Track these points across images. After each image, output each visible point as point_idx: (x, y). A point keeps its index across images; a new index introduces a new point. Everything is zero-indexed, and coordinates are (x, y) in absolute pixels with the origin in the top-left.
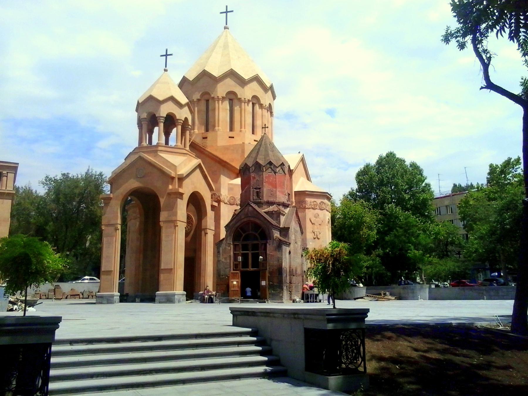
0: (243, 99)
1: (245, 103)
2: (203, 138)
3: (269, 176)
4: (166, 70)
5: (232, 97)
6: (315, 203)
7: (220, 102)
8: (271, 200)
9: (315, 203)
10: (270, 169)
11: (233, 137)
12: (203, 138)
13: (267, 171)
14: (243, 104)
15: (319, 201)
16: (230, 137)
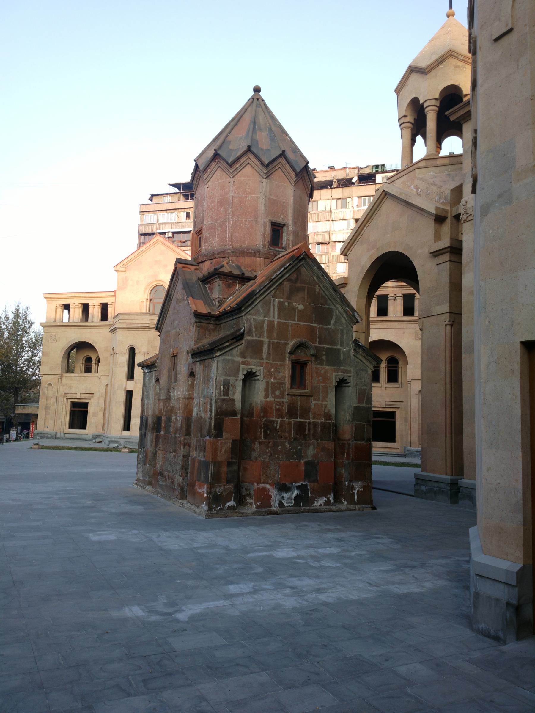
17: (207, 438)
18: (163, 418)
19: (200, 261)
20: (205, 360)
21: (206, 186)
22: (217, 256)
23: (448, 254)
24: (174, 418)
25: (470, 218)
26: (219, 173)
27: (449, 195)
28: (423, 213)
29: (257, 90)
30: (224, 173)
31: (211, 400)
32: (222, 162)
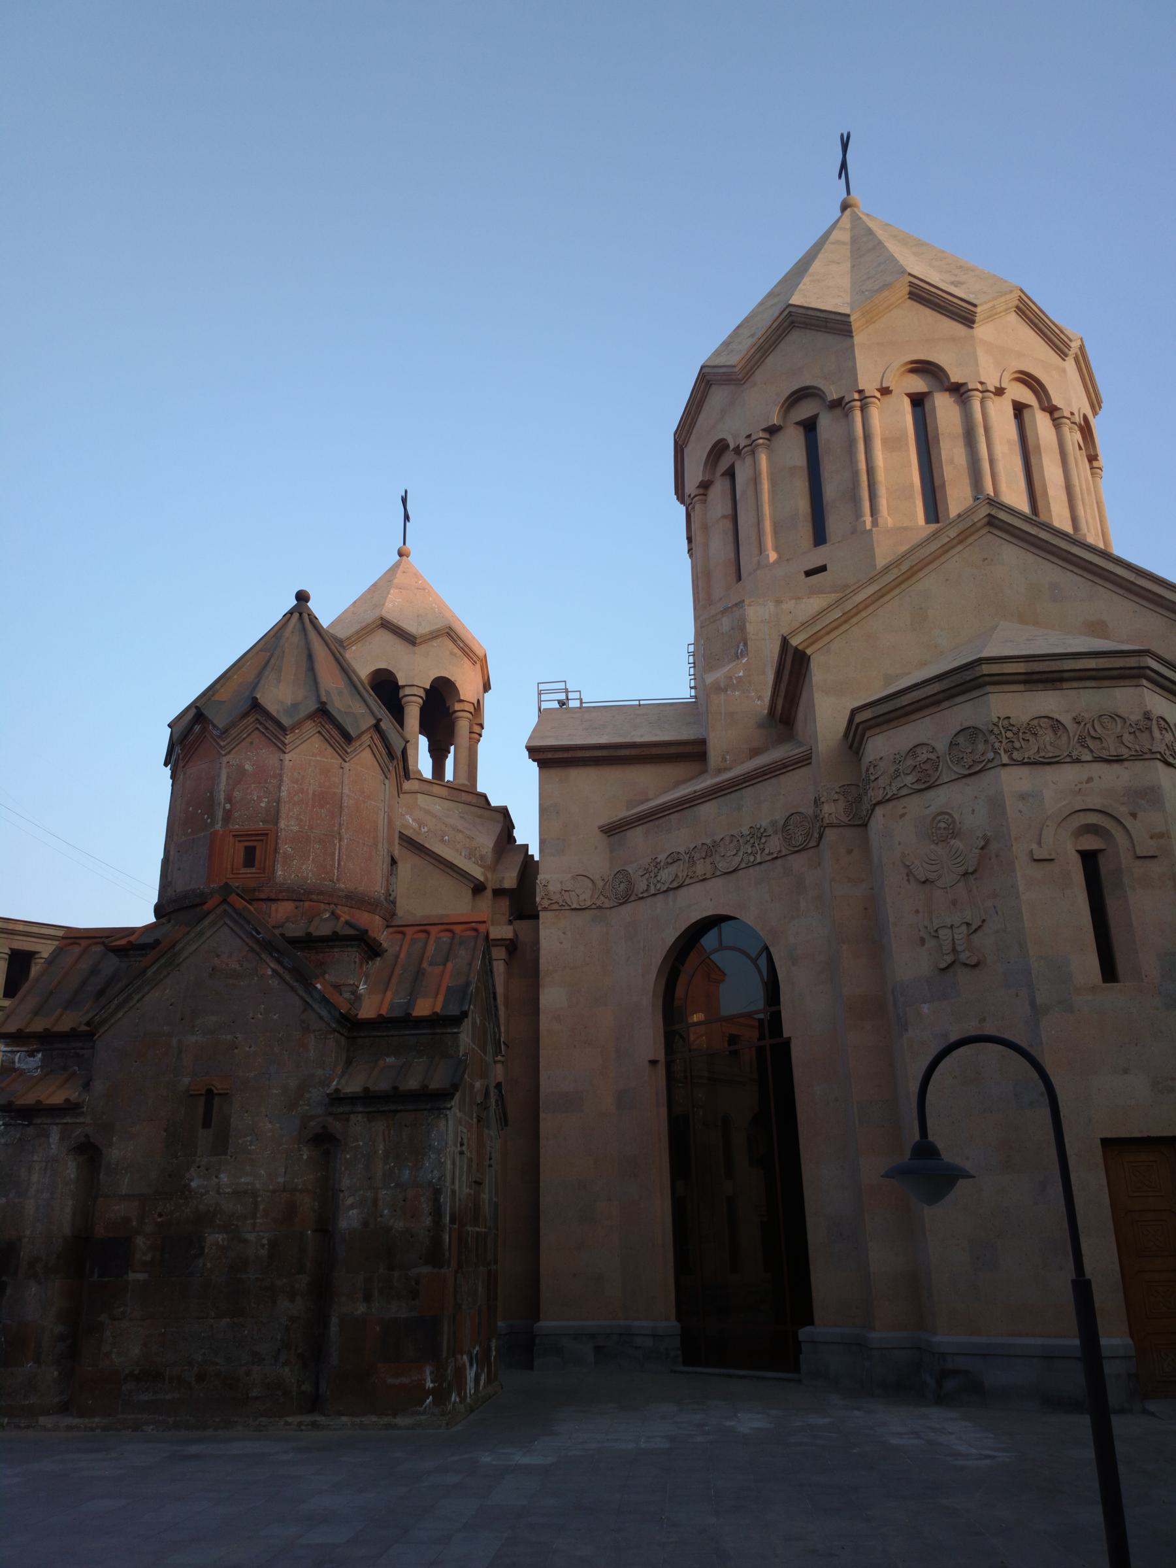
4: (401, 554)
17: (425, 1270)
18: (140, 1241)
19: (262, 896)
20: (401, 1111)
21: (287, 757)
22: (314, 897)
23: (503, 949)
24: (215, 1238)
25: (555, 907)
26: (317, 743)
27: (490, 855)
28: (449, 870)
29: (302, 597)
30: (330, 749)
31: (437, 1192)
32: (329, 726)
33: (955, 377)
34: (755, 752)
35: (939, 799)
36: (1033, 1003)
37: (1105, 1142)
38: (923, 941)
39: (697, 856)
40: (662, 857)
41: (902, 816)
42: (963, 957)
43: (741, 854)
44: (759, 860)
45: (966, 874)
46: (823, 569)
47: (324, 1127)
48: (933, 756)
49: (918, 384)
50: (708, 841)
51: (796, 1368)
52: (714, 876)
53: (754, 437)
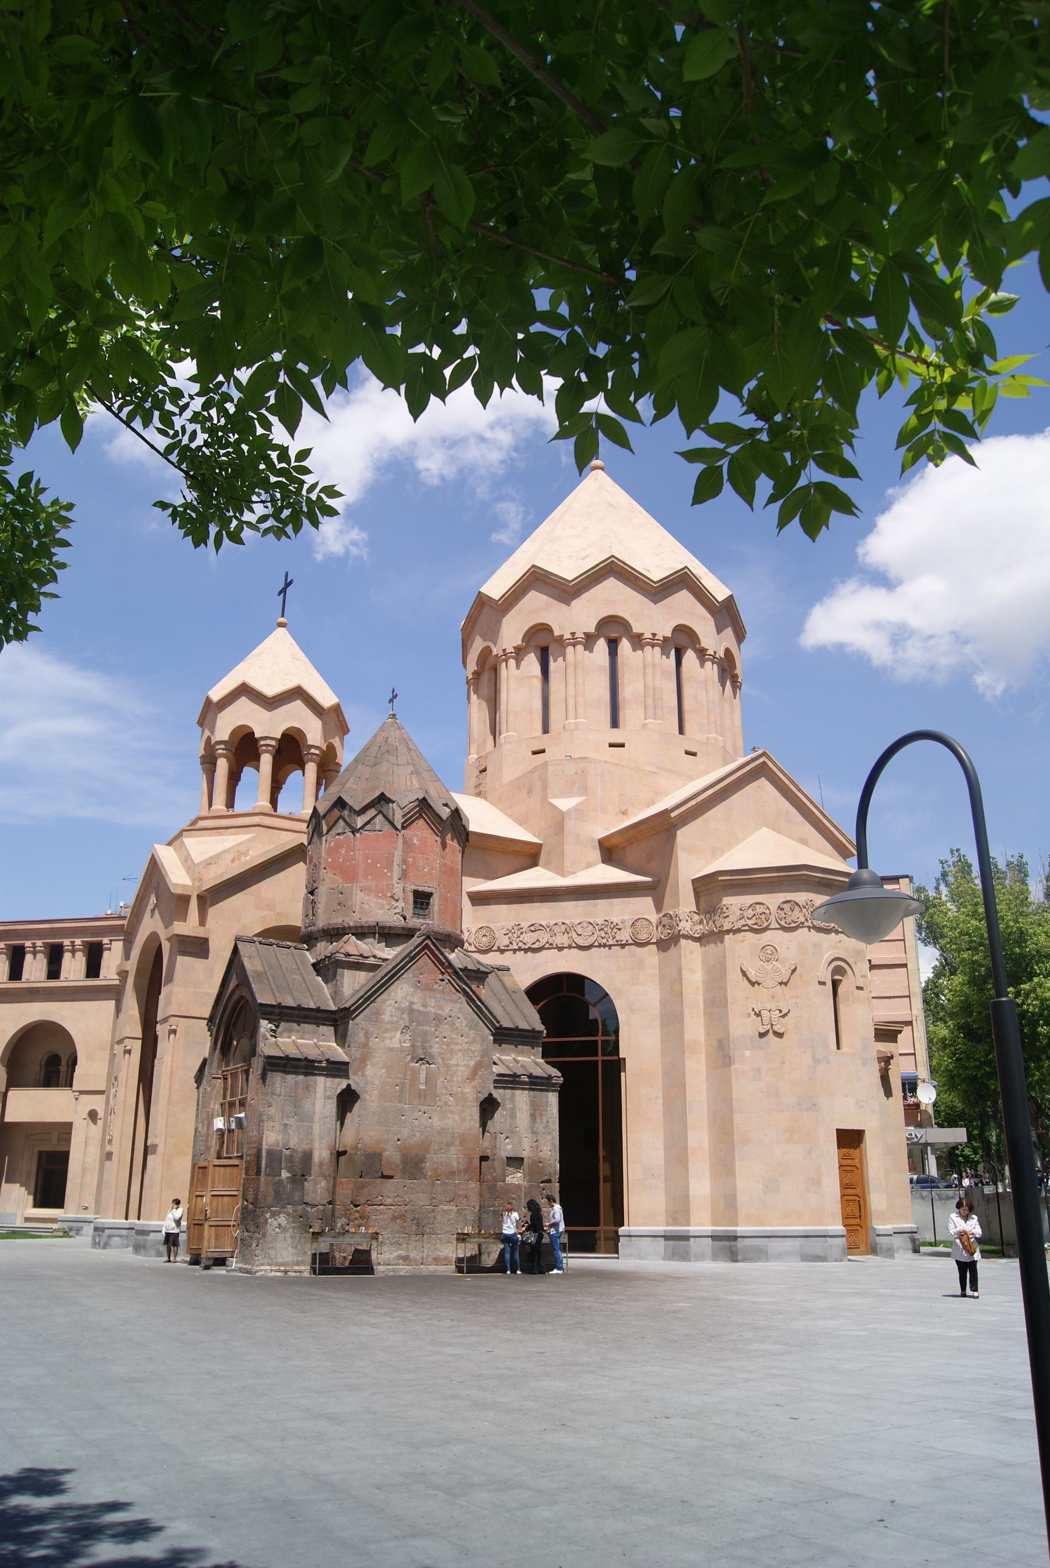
0: (567, 636)
1: (574, 645)
2: (481, 772)
3: (339, 845)
5: (541, 640)
6: (760, 909)
7: (512, 662)
8: (338, 920)
9: (760, 909)
10: (341, 823)
11: (543, 751)
12: (481, 772)
13: (333, 832)
14: (570, 649)
15: (773, 900)
16: (535, 753)
33: (703, 644)
34: (590, 865)
35: (768, 937)
36: (814, 1057)
37: (840, 1132)
38: (749, 1015)
39: (556, 929)
40: (525, 925)
41: (742, 941)
42: (775, 1028)
43: (596, 935)
44: (611, 942)
45: (781, 984)
46: (622, 745)
47: (490, 1094)
48: (767, 911)
49: (683, 640)
50: (567, 922)
51: (617, 1253)
52: (570, 947)
53: (576, 636)
